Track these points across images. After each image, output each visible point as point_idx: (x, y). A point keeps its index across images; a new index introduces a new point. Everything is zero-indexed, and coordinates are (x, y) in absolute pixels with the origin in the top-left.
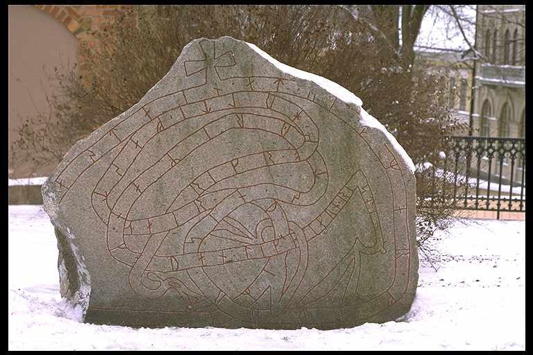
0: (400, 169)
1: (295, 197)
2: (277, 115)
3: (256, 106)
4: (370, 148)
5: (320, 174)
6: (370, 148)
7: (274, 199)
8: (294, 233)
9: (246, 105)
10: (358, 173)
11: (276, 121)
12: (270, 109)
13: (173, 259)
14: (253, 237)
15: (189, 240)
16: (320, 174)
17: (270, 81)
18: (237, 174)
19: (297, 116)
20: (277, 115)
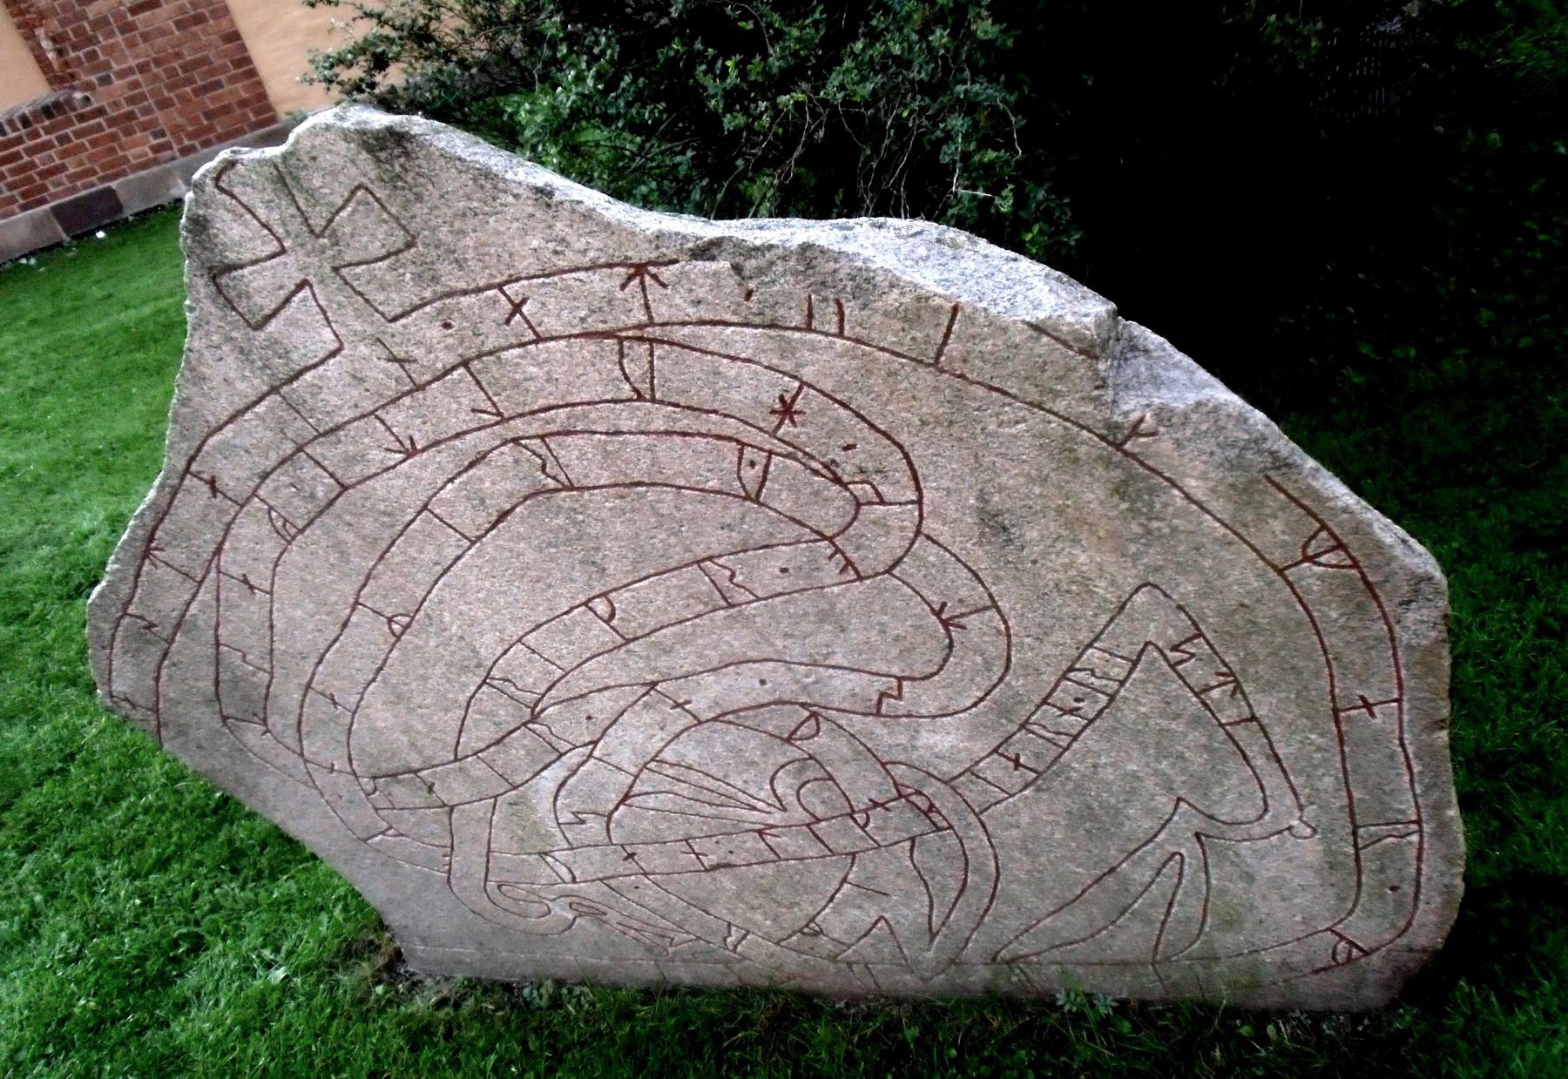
0: (1355, 565)
1: (882, 695)
2: (686, 422)
3: (585, 397)
4: (1188, 497)
5: (962, 615)
6: (1188, 497)
7: (803, 705)
8: (919, 793)
9: (541, 403)
10: (1139, 598)
11: (700, 443)
12: (653, 400)
13: (549, 859)
14: (772, 809)
15: (566, 817)
16: (962, 615)
17: (601, 283)
18: (628, 641)
19: (786, 410)
20: (686, 422)
